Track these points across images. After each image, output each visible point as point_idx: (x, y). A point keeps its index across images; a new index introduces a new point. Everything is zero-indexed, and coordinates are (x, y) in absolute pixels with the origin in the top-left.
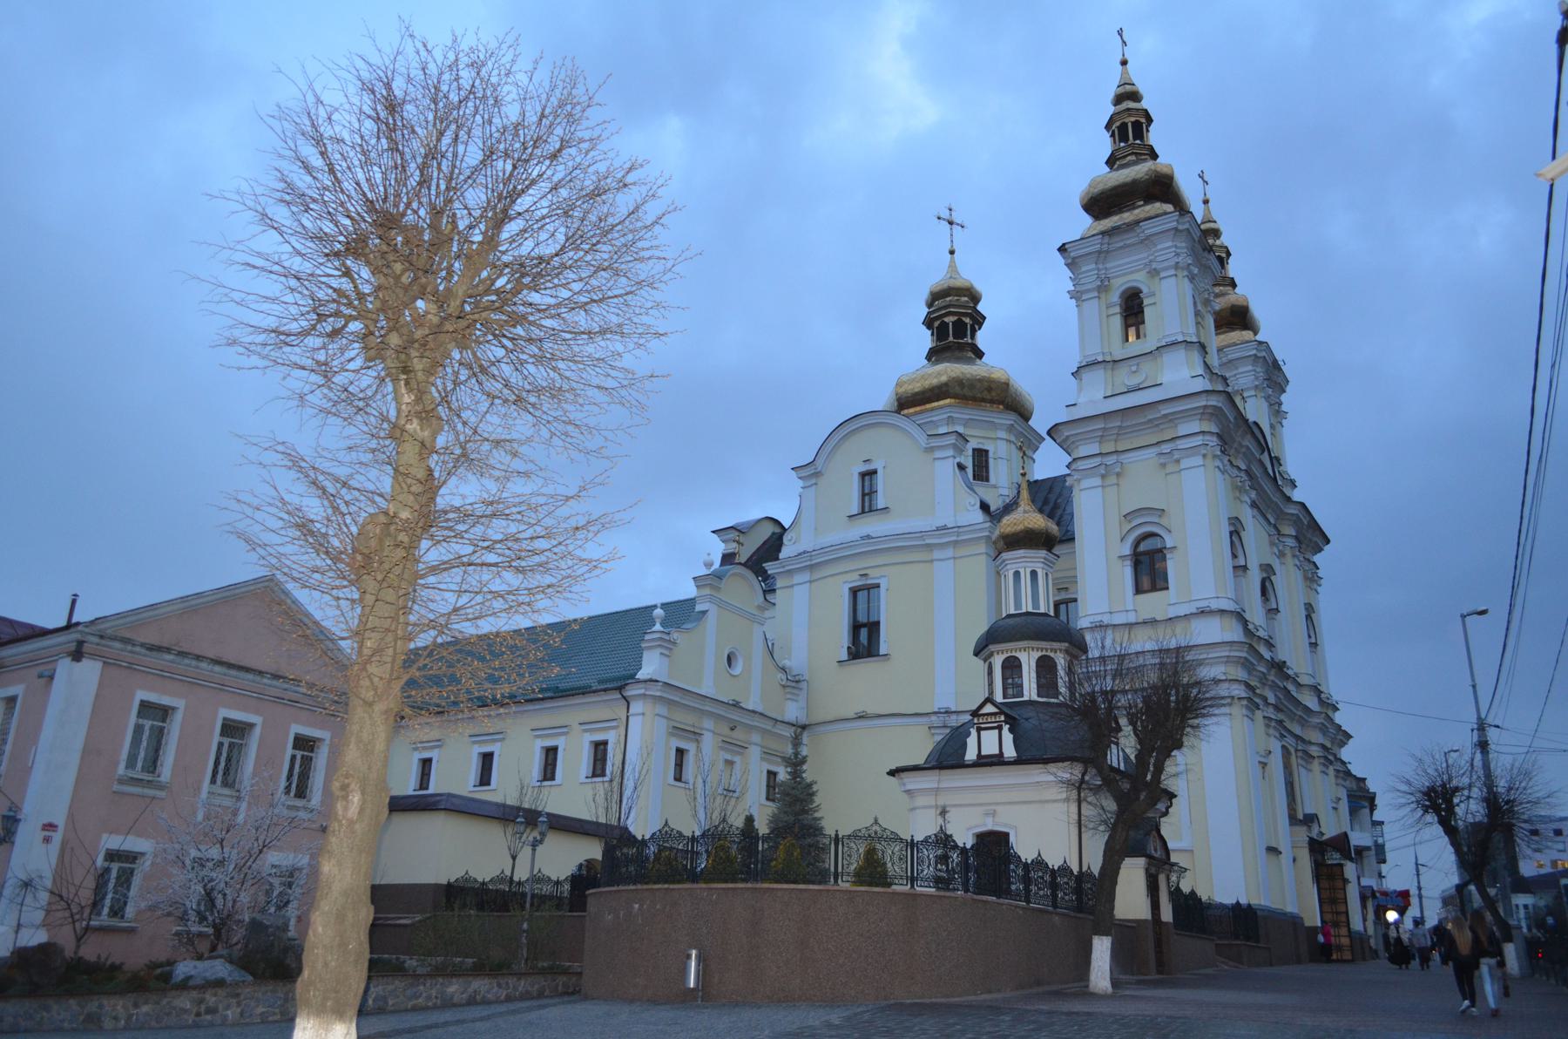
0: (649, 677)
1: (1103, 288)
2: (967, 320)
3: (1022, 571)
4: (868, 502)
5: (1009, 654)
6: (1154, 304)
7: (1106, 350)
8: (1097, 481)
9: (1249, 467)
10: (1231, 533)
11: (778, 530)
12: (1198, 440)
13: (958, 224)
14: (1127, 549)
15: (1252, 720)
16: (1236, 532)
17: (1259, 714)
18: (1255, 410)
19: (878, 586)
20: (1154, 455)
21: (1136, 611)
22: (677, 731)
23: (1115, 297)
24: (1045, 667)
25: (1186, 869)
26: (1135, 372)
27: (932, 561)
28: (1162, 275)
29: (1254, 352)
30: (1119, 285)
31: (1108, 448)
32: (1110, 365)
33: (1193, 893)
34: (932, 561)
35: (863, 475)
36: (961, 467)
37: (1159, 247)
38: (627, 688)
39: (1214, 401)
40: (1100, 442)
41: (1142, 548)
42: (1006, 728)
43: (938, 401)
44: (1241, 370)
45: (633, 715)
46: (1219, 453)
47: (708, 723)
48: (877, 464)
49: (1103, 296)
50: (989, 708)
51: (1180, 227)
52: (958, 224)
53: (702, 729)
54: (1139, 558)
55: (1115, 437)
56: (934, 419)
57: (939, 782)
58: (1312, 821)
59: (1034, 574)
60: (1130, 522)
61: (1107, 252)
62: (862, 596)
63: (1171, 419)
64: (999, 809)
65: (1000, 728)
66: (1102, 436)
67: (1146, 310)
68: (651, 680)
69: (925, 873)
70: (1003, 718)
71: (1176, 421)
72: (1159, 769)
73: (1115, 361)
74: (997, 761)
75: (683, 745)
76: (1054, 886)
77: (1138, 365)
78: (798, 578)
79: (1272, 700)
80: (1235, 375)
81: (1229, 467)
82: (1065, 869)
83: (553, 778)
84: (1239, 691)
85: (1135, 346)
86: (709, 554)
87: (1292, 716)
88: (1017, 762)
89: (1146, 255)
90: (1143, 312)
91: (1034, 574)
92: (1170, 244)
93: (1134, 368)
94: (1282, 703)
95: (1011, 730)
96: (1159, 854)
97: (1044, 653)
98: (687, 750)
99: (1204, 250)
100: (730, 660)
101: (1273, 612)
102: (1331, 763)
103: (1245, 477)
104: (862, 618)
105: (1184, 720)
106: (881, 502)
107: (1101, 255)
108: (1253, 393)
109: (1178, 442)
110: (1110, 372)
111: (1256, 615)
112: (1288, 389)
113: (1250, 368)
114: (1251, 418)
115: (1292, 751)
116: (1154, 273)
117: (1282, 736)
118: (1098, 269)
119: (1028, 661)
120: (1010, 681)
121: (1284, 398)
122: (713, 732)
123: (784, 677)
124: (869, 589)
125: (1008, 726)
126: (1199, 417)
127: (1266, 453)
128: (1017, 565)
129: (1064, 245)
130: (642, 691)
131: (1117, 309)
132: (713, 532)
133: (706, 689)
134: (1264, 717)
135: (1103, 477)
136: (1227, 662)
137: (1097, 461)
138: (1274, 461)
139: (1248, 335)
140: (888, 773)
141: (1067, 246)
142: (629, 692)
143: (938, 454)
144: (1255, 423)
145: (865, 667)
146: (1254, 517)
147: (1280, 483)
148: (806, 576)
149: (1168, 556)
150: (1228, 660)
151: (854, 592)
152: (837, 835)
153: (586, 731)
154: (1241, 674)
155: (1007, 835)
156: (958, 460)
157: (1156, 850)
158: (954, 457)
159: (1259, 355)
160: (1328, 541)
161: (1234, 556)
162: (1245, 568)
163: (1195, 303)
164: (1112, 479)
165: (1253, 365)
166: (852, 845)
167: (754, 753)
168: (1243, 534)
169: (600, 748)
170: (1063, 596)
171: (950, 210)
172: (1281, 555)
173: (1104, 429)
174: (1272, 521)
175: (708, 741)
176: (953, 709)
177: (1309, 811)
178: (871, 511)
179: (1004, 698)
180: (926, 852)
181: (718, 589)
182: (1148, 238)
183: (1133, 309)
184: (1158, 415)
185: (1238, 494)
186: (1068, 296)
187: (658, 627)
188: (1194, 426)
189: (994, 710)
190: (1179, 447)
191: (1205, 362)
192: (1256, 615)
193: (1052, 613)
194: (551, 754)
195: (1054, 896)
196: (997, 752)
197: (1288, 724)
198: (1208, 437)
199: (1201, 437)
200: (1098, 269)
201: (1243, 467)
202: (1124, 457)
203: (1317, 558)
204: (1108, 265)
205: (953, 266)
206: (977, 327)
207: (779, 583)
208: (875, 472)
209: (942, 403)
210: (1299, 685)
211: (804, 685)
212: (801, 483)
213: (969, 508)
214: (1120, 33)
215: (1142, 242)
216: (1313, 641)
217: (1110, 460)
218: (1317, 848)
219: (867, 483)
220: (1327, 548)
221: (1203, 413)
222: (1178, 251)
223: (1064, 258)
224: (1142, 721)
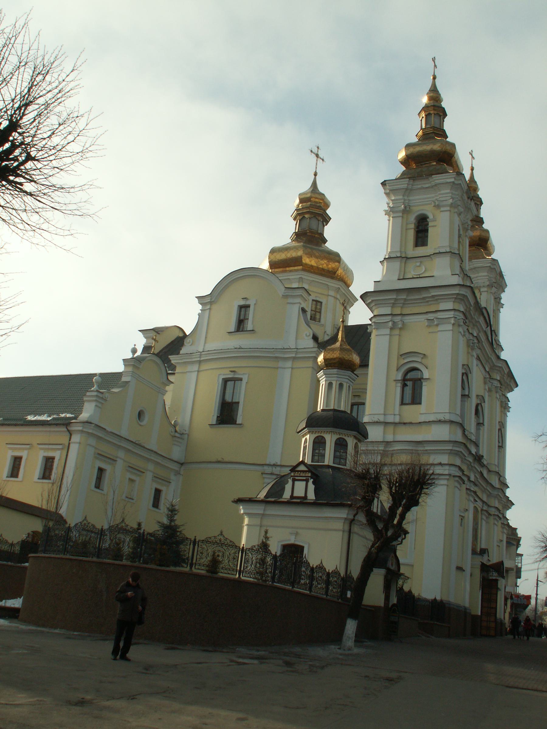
0: (86, 420)
1: (406, 211)
3: (334, 383)
5: (319, 435)
6: (435, 226)
7: (403, 250)
8: (388, 331)
9: (478, 334)
10: (463, 374)
11: (181, 335)
12: (451, 314)
13: (321, 158)
14: (400, 376)
15: (460, 490)
16: (466, 375)
17: (464, 486)
18: (484, 299)
19: (241, 380)
20: (423, 320)
21: (400, 415)
22: (100, 456)
23: (412, 219)
24: (341, 445)
25: (408, 578)
26: (419, 266)
27: (277, 368)
28: (442, 209)
29: (489, 265)
30: (418, 210)
31: (397, 311)
32: (404, 259)
33: (410, 592)
34: (277, 368)
35: (241, 307)
36: (304, 310)
37: (442, 192)
38: (71, 425)
39: (463, 291)
40: (392, 307)
41: (409, 376)
42: (311, 481)
43: (294, 266)
44: (480, 274)
45: (73, 443)
46: (462, 324)
47: (121, 454)
48: (251, 302)
49: (405, 216)
50: (302, 468)
51: (456, 182)
52: (321, 158)
53: (117, 457)
54: (406, 382)
55: (401, 305)
56: (290, 277)
57: (264, 510)
58: (484, 553)
59: (341, 385)
60: (404, 359)
61: (411, 190)
62: (230, 384)
63: (437, 299)
64: (300, 531)
65: (307, 481)
66: (393, 304)
67: (430, 230)
68: (87, 422)
69: (248, 568)
70: (310, 475)
71: (440, 301)
72: (403, 517)
73: (407, 258)
74: (302, 502)
75: (103, 466)
76: (328, 583)
77: (421, 262)
78: (190, 368)
79: (472, 479)
80: (476, 277)
81: (467, 333)
82: (336, 573)
83: (16, 476)
84: (455, 472)
85: (421, 251)
86: (135, 345)
87: (484, 490)
88: (314, 504)
89: (433, 195)
90: (427, 231)
92: (448, 191)
93: (418, 264)
94: (478, 481)
95: (314, 483)
96: (393, 567)
97: (341, 436)
98: (105, 470)
99: (468, 198)
100: (140, 415)
101: (479, 424)
102: (500, 518)
103: (476, 341)
104: (228, 399)
105: (422, 488)
107: (408, 191)
108: (485, 289)
109: (439, 313)
110: (403, 264)
111: (471, 427)
112: (506, 290)
113: (486, 274)
114: (483, 304)
115: (479, 509)
116: (438, 207)
117: (475, 501)
118: (405, 200)
119: (330, 439)
120: (317, 451)
122: (124, 461)
123: (173, 430)
124: (235, 381)
125: (312, 480)
126: (453, 300)
127: (489, 327)
128: (332, 379)
129: (385, 181)
130: (80, 428)
131: (412, 226)
132: (140, 331)
133: (124, 433)
134: (467, 489)
135: (391, 329)
136: (450, 453)
138: (493, 333)
139: (488, 252)
140: (233, 502)
141: (387, 182)
142: (73, 428)
143: (290, 300)
144: (485, 308)
145: (227, 431)
146: (477, 365)
147: (495, 346)
148: (196, 367)
149: (424, 384)
150: (451, 453)
151: (226, 381)
152: (195, 539)
153: (41, 449)
154: (458, 462)
155: (302, 548)
156: (302, 306)
157: (392, 565)
158: (300, 303)
159: (492, 267)
160: (517, 385)
161: (463, 388)
162: (468, 396)
163: (459, 230)
164: (397, 332)
165: (488, 273)
166: (204, 546)
167: (149, 476)
168: (469, 375)
169: (49, 462)
170: (357, 400)
171: (318, 148)
172: (490, 390)
173: (396, 300)
174: (487, 369)
175: (120, 464)
176: (279, 463)
177: (483, 546)
178: (242, 331)
179: (312, 462)
180: (251, 556)
181: (138, 368)
182: (436, 185)
184: (430, 295)
185: (470, 351)
186: (384, 213)
187: (95, 388)
188: (449, 305)
189: (305, 469)
190: (439, 317)
191: (460, 266)
192: (471, 426)
193: (349, 412)
194: (17, 461)
195: (327, 589)
196: (303, 495)
197: (479, 493)
198: (457, 313)
199: (452, 313)
200: (405, 200)
201: (475, 335)
202: (407, 319)
204: (411, 198)
205: (314, 184)
206: (325, 223)
207: (178, 370)
208: (248, 306)
209: (296, 268)
210: (489, 471)
211: (186, 436)
212: (200, 307)
213: (306, 338)
214: (434, 60)
215: (432, 187)
216: (500, 445)
217: (397, 319)
218: (484, 568)
219: (242, 313)
220: (516, 389)
221: (456, 298)
222: (454, 196)
223: (384, 189)
224: (396, 487)
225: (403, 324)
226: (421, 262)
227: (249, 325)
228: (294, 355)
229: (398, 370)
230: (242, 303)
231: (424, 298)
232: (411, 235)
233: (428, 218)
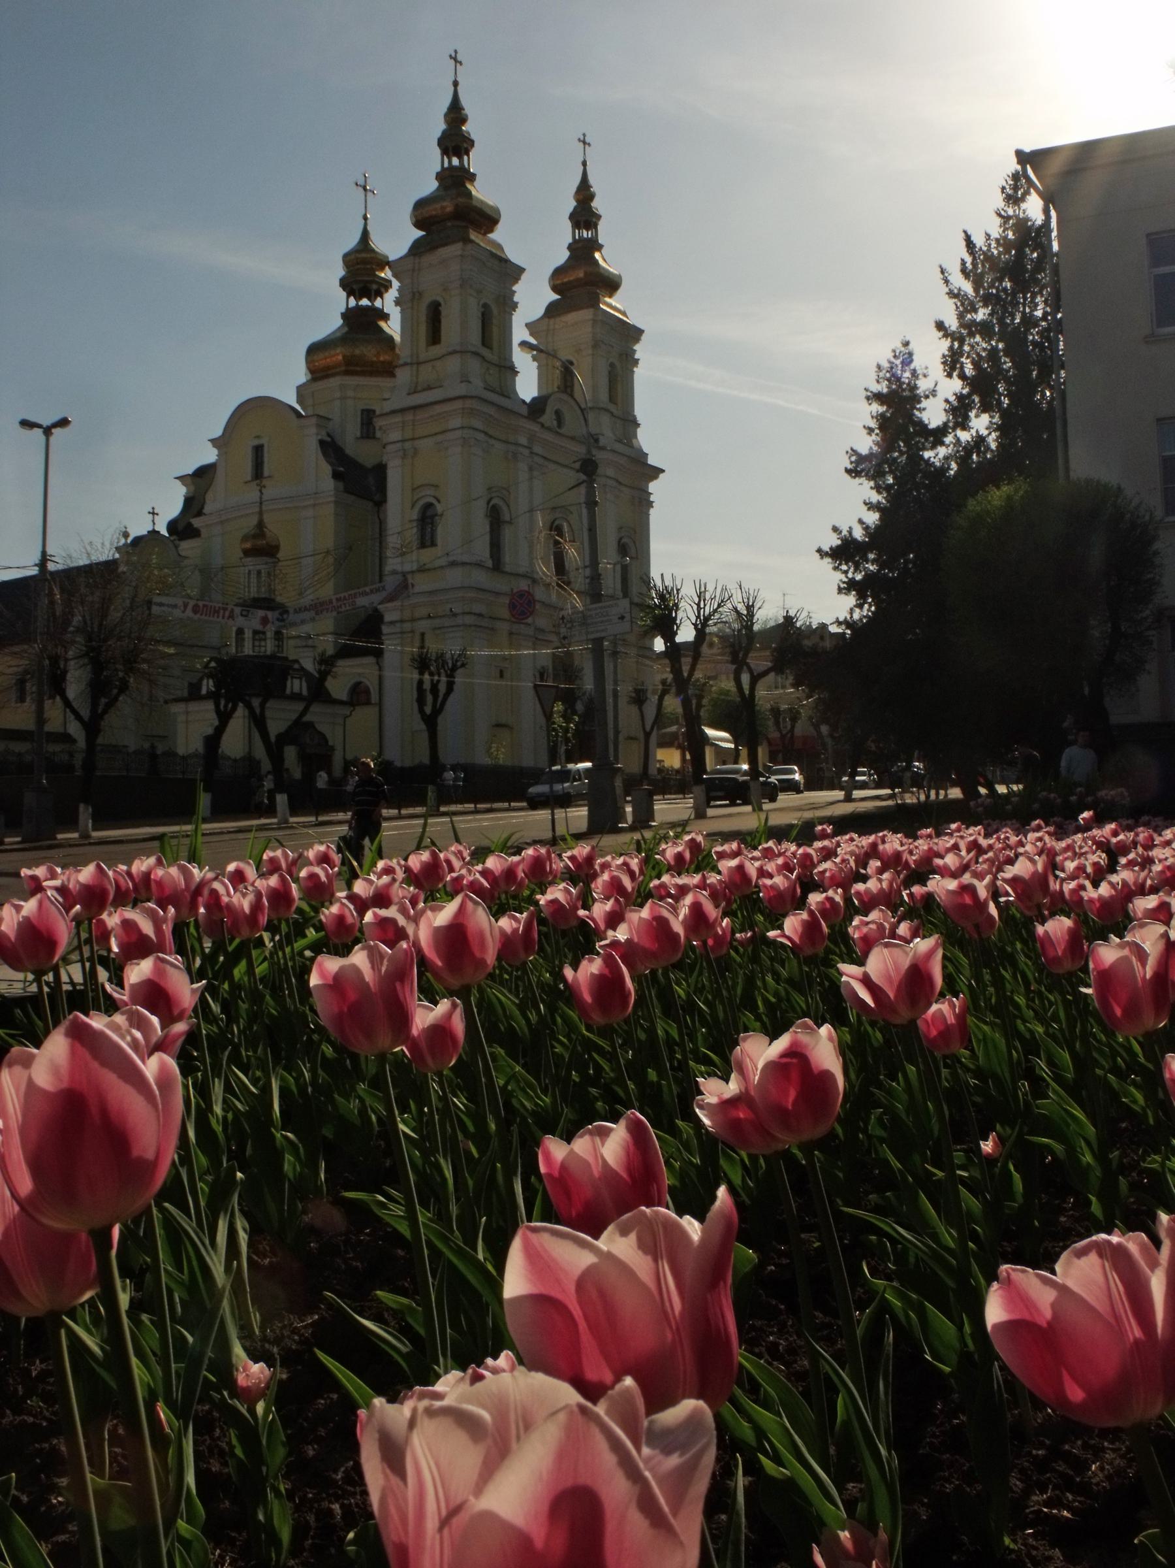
2: (375, 287)
4: (258, 472)
12: (458, 433)
14: (415, 514)
32: (415, 367)
40: (403, 430)
48: (264, 441)
59: (259, 572)
90: (439, 322)
91: (259, 572)
106: (266, 473)
121: (636, 347)
131: (423, 318)
135: (403, 458)
137: (399, 445)
156: (319, 437)
183: (435, 314)
203: (653, 487)
205: (365, 235)
206: (383, 290)
217: (408, 445)
225: (415, 449)
226: (433, 367)
227: (266, 473)
228: (312, 502)
229: (413, 506)
230: (257, 442)
231: (431, 416)
232: (423, 329)
233: (439, 305)
